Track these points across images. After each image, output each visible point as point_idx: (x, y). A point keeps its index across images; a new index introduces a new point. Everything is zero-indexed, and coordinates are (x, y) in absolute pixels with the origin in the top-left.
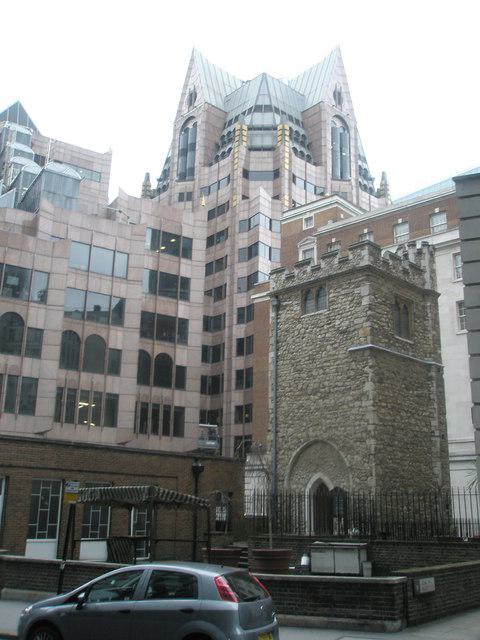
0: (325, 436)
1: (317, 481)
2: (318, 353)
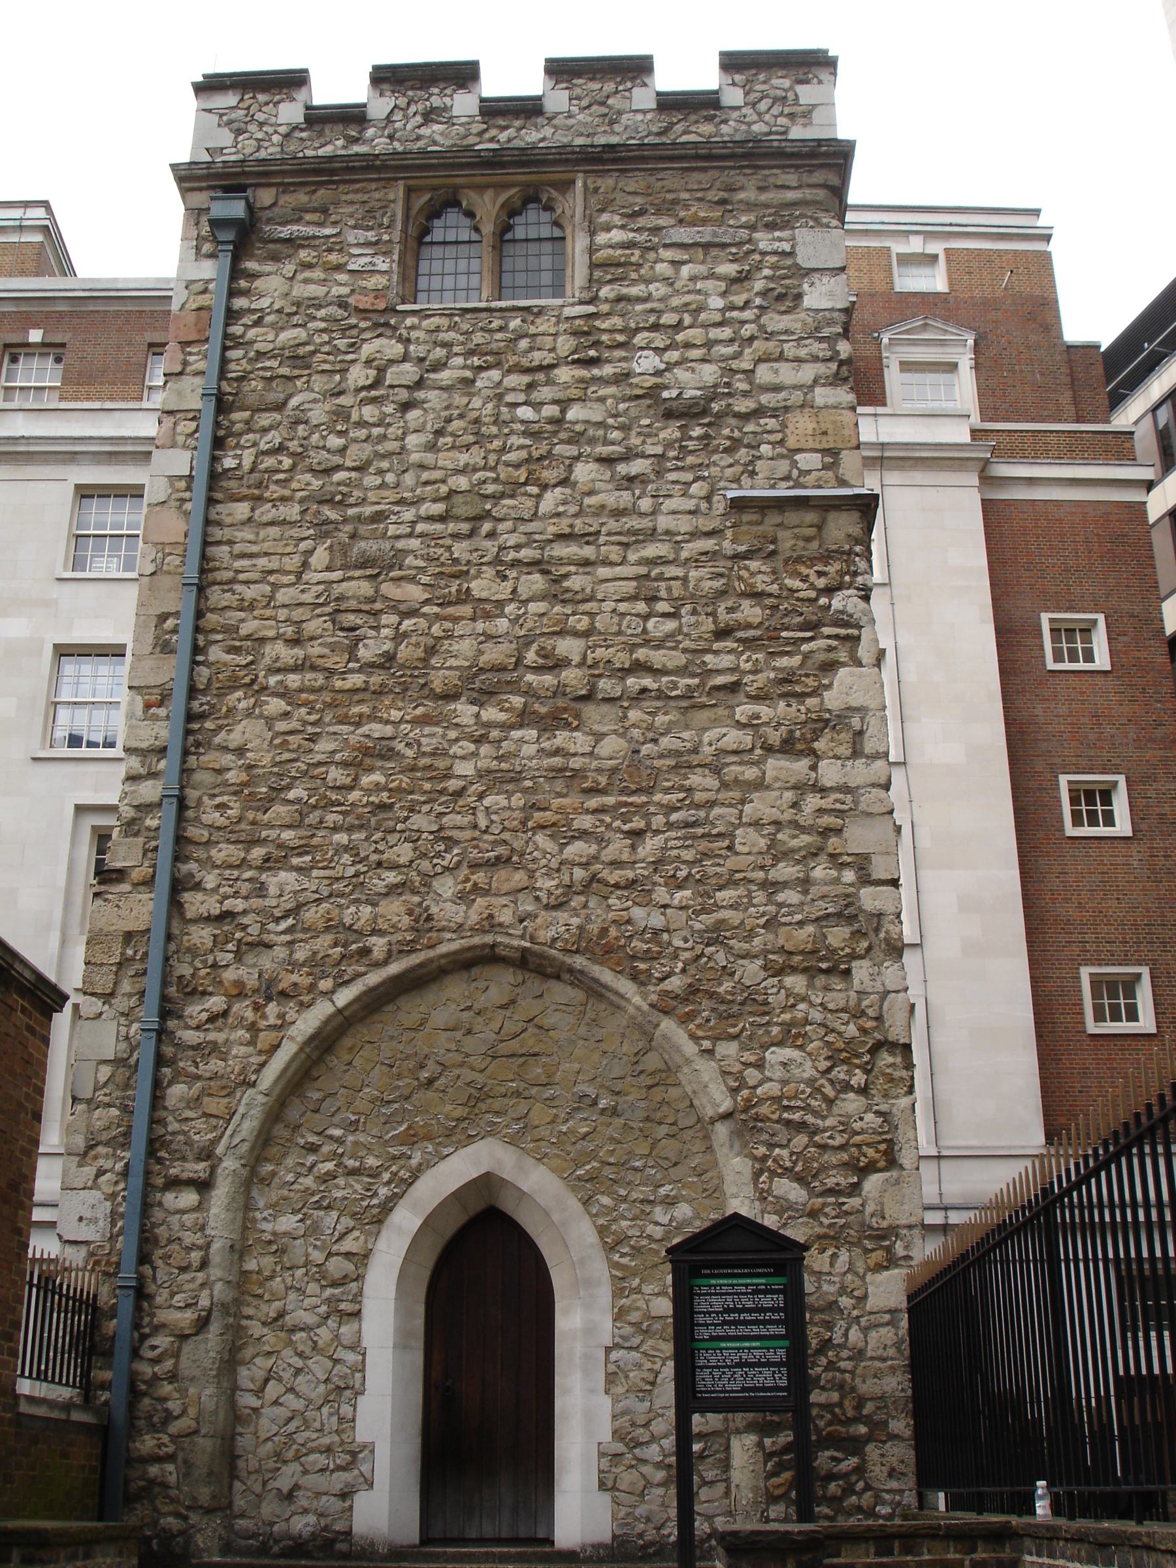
2: (513, 489)
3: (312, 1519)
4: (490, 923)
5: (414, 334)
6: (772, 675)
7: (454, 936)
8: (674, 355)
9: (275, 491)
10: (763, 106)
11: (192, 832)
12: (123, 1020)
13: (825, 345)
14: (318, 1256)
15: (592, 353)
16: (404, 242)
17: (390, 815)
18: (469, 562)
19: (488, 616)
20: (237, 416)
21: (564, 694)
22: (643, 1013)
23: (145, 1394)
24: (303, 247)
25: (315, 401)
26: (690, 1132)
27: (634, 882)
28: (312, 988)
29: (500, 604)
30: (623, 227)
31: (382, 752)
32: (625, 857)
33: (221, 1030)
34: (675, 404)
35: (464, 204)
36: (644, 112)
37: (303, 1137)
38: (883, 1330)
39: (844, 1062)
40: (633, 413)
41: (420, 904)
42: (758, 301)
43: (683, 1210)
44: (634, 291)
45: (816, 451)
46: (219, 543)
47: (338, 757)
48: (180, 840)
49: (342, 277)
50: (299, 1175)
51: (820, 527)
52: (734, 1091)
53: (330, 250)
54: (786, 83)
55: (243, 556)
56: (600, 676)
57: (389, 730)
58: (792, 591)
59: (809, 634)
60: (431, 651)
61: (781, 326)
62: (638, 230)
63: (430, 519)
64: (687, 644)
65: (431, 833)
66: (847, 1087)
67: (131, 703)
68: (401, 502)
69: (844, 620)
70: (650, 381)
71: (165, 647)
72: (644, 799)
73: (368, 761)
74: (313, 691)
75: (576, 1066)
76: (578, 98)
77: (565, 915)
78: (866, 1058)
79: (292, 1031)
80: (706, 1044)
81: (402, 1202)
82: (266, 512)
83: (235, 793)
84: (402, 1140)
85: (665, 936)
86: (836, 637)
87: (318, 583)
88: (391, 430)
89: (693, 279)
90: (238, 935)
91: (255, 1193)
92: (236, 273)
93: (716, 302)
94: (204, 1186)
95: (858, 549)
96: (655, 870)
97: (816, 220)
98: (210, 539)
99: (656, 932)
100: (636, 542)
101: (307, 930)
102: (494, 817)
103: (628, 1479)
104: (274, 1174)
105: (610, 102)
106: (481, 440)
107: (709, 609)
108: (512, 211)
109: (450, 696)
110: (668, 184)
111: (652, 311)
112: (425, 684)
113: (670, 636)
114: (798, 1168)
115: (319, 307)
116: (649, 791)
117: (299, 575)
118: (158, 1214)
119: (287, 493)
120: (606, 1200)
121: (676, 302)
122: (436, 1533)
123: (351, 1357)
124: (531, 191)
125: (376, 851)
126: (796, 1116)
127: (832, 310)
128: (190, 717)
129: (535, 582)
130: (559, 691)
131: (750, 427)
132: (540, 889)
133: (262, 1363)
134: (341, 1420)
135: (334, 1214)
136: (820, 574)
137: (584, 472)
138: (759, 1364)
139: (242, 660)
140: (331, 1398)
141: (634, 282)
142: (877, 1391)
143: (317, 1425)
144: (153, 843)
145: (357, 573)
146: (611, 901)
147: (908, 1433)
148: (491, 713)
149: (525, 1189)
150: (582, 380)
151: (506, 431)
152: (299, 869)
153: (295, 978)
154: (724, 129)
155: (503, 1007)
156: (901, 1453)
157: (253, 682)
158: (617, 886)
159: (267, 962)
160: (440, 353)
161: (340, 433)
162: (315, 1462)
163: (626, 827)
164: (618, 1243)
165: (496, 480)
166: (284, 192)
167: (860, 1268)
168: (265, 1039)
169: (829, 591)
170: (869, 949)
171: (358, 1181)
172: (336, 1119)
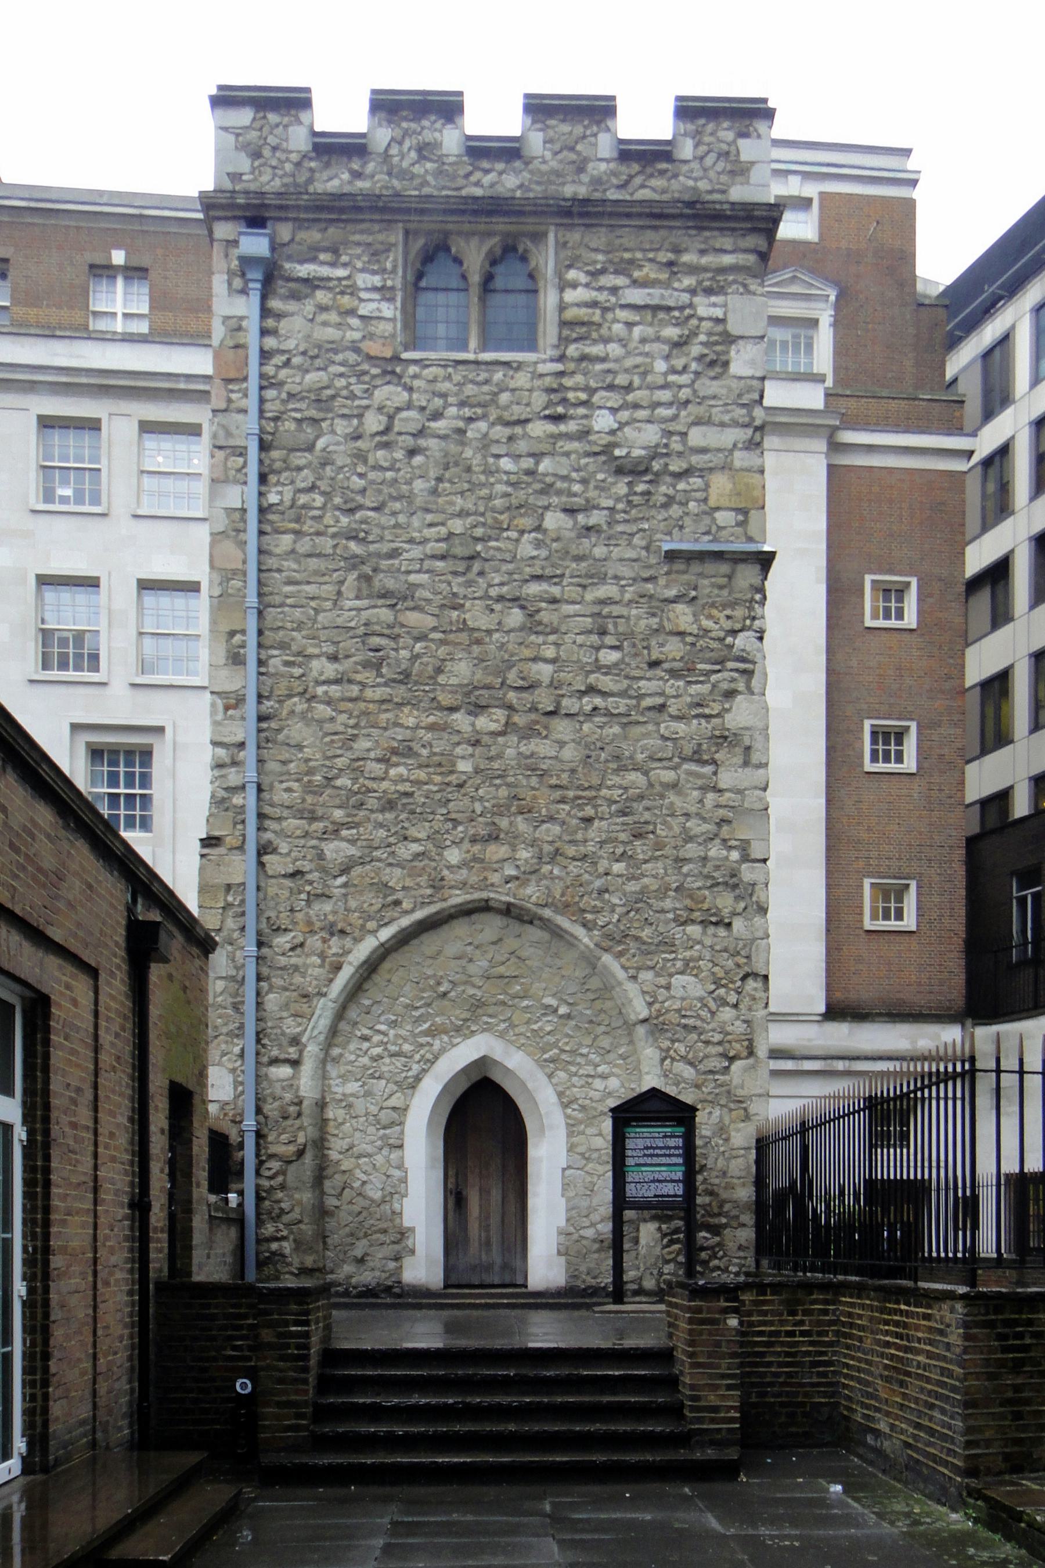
1: (465, 1071)
4: (485, 885)
5: (416, 383)
6: (689, 699)
7: (458, 892)
8: (624, 415)
9: (308, 526)
10: (709, 161)
11: (267, 810)
13: (744, 411)
14: (373, 1109)
15: (560, 410)
17: (411, 800)
18: (465, 596)
20: (275, 454)
21: (537, 710)
22: (591, 950)
23: (264, 1199)
24: (318, 287)
25: (338, 444)
26: (619, 1031)
28: (363, 926)
29: (489, 632)
30: (587, 285)
31: (404, 751)
35: (453, 250)
36: (607, 161)
38: (740, 1160)
39: (723, 986)
40: (591, 468)
41: (435, 869)
42: (694, 366)
43: (614, 1083)
44: (596, 350)
47: (372, 755)
48: (261, 816)
49: (354, 322)
51: (730, 577)
52: (650, 1004)
53: (342, 293)
54: (729, 136)
55: (290, 582)
56: (563, 696)
58: (707, 631)
59: (718, 667)
60: (439, 671)
61: (710, 392)
62: (600, 289)
63: (434, 557)
66: (725, 1003)
67: (213, 705)
68: (411, 541)
70: (607, 439)
71: (236, 659)
72: (593, 793)
73: (394, 759)
74: (351, 700)
75: (544, 985)
79: (350, 958)
80: (632, 972)
82: (304, 546)
83: (297, 780)
84: (428, 1033)
85: (607, 896)
86: (737, 670)
87: (350, 610)
88: (402, 473)
89: (643, 341)
90: (308, 888)
91: (329, 1067)
92: (265, 312)
93: (660, 366)
94: (295, 1063)
95: (758, 597)
97: (745, 286)
98: (264, 568)
101: (356, 886)
102: (487, 804)
104: (341, 1055)
105: (579, 147)
107: (645, 644)
109: (452, 709)
110: (626, 242)
111: (609, 371)
112: (434, 699)
113: (616, 665)
114: (690, 1056)
115: (336, 352)
119: (322, 528)
120: (562, 1074)
121: (629, 363)
122: (452, 1281)
123: (397, 1173)
126: (691, 1022)
127: (752, 378)
128: (261, 718)
129: (515, 617)
131: (681, 486)
135: (383, 1082)
136: (728, 617)
137: (553, 520)
139: (297, 671)
141: (595, 342)
144: (240, 817)
145: (380, 602)
147: (752, 1222)
148: (483, 723)
149: (510, 1066)
150: (552, 436)
151: (492, 480)
152: (348, 841)
154: (675, 185)
155: (494, 943)
156: (746, 1235)
157: (305, 691)
158: (574, 859)
159: (327, 907)
160: (438, 402)
161: (361, 476)
163: (580, 814)
164: (571, 1102)
165: (484, 524)
166: (300, 228)
167: (727, 1121)
169: (734, 632)
170: (745, 908)
172: (382, 1019)
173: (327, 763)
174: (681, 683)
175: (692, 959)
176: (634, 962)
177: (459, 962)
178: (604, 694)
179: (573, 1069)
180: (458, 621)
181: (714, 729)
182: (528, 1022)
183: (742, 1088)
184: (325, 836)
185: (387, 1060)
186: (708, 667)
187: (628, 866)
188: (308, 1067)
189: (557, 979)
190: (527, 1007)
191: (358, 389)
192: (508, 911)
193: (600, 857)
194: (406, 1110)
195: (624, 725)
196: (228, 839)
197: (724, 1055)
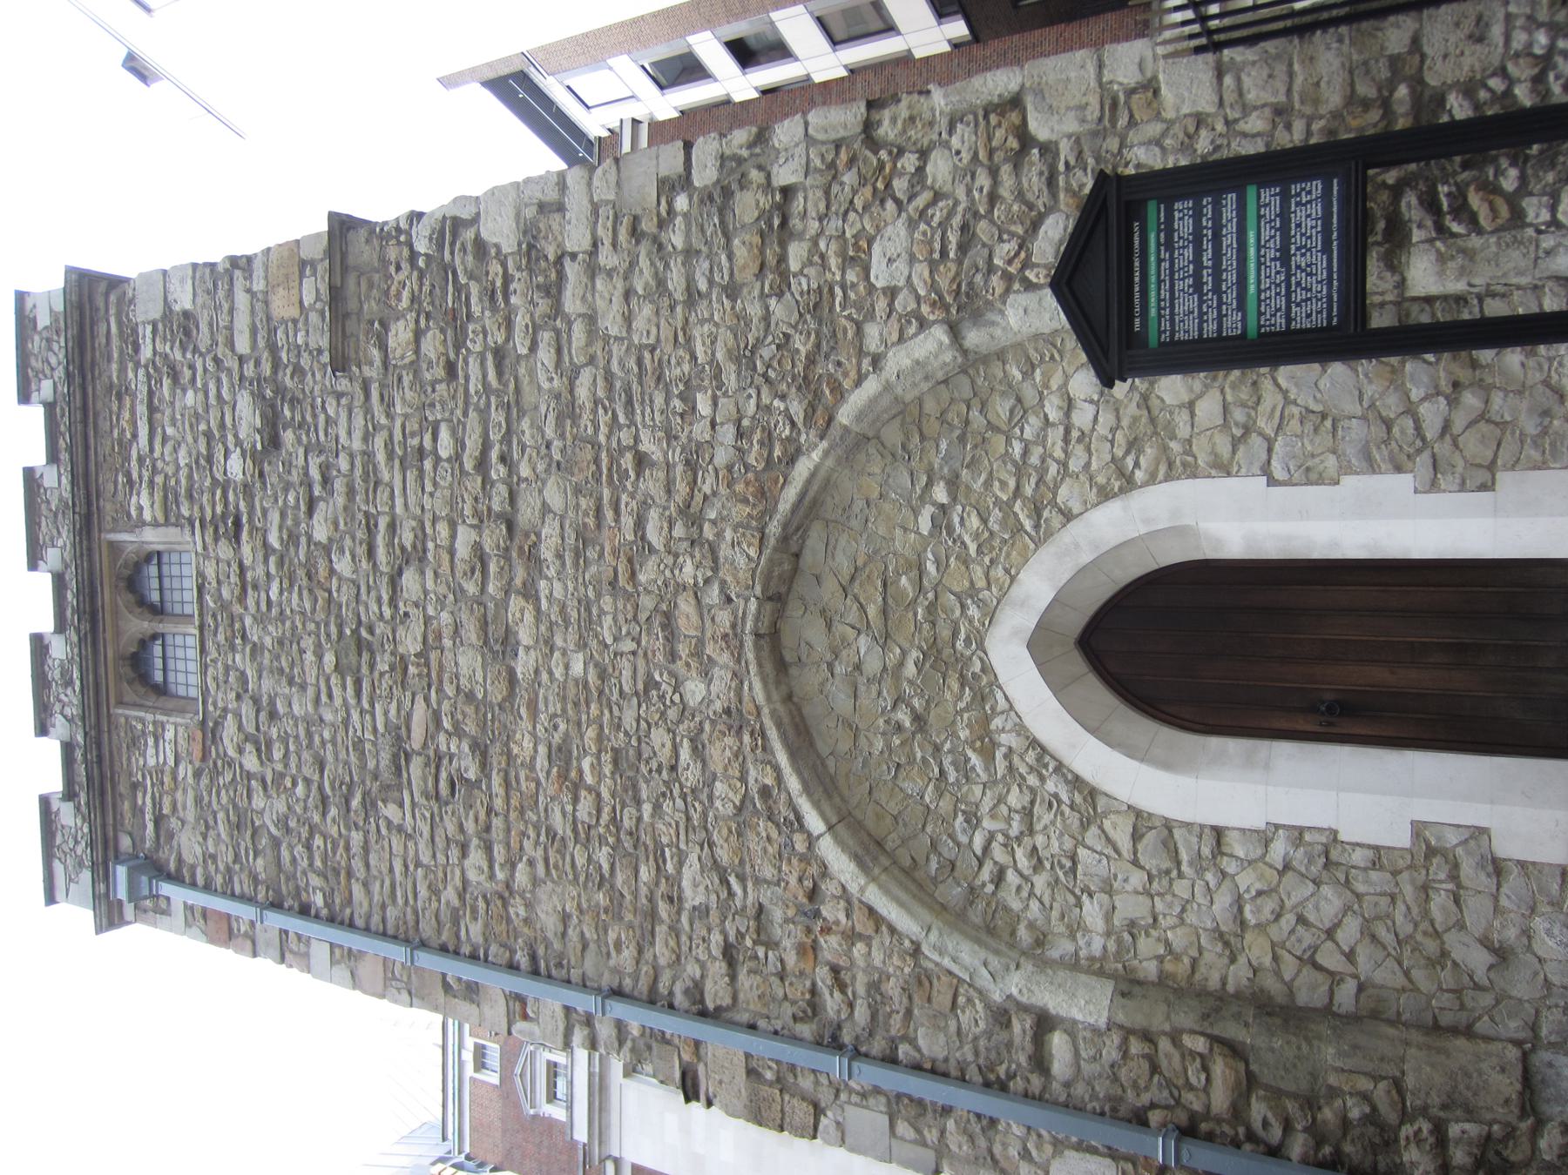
0: (740, 557)
1: (1058, 687)
3: (1539, 924)
4: (731, 639)
5: (220, 704)
6: (487, 313)
7: (746, 684)
12: (843, 1096)
14: (1137, 879)
16: (154, 709)
18: (393, 653)
19: (439, 637)
26: (980, 381)
27: (687, 463)
28: (804, 859)
29: (427, 620)
31: (562, 755)
32: (661, 475)
33: (854, 978)
34: (266, 436)
36: (60, 475)
37: (984, 885)
38: (1247, 81)
39: (888, 185)
40: (275, 479)
41: (713, 722)
42: (189, 356)
45: (301, 284)
46: (384, 920)
47: (569, 808)
50: (1031, 894)
52: (923, 324)
56: (489, 509)
57: (542, 750)
60: (470, 696)
64: (459, 412)
65: (639, 706)
69: (438, 238)
71: (472, 991)
72: (604, 455)
73: (573, 774)
74: (508, 830)
75: (898, 532)
76: (52, 539)
77: (723, 546)
78: (883, 154)
79: (853, 888)
80: (866, 364)
81: (1066, 762)
85: (746, 423)
86: (453, 244)
90: (749, 942)
91: (1054, 954)
94: (1044, 1023)
96: (676, 438)
99: (740, 434)
100: (375, 474)
101: (742, 862)
103: (1475, 445)
104: (1031, 926)
106: (296, 638)
108: (142, 602)
112: (500, 706)
113: (453, 432)
114: (1020, 230)
116: (596, 446)
117: (409, 836)
118: (1080, 1090)
119: (342, 843)
120: (1063, 492)
123: (1279, 849)
124: (122, 584)
125: (659, 771)
126: (953, 238)
129: (409, 579)
130: (506, 554)
132: (695, 577)
133: (1289, 967)
134: (1376, 864)
135: (1082, 852)
136: (398, 268)
138: (1285, 230)
140: (1342, 878)
142: (1340, 79)
143: (1384, 902)
145: (405, 775)
146: (709, 492)
149: (1052, 596)
150: (250, 533)
151: (288, 612)
152: (681, 864)
153: (793, 880)
157: (501, 897)
159: (777, 914)
161: (294, 784)
162: (1443, 908)
163: (632, 474)
164: (1121, 473)
167: (1155, 129)
168: (862, 925)
169: (414, 256)
170: (760, 168)
171: (1039, 819)
172: (964, 839)
173: (582, 879)
174: (471, 327)
175: (842, 254)
176: (850, 365)
177: (862, 688)
178: (486, 446)
179: (1053, 469)
180: (418, 665)
181: (519, 269)
182: (965, 561)
183: (1082, 107)
184: (675, 900)
185: (1040, 840)
186: (450, 288)
187: (700, 388)
188: (1053, 1000)
189: (887, 506)
190: (937, 562)
191: (228, 777)
192: (777, 598)
193: (690, 439)
194: (1138, 814)
195: (522, 413)
196: (686, 1057)
197: (1018, 159)
